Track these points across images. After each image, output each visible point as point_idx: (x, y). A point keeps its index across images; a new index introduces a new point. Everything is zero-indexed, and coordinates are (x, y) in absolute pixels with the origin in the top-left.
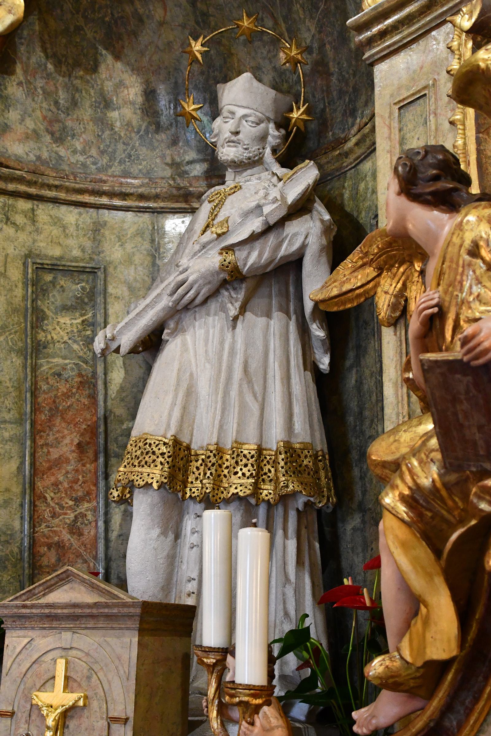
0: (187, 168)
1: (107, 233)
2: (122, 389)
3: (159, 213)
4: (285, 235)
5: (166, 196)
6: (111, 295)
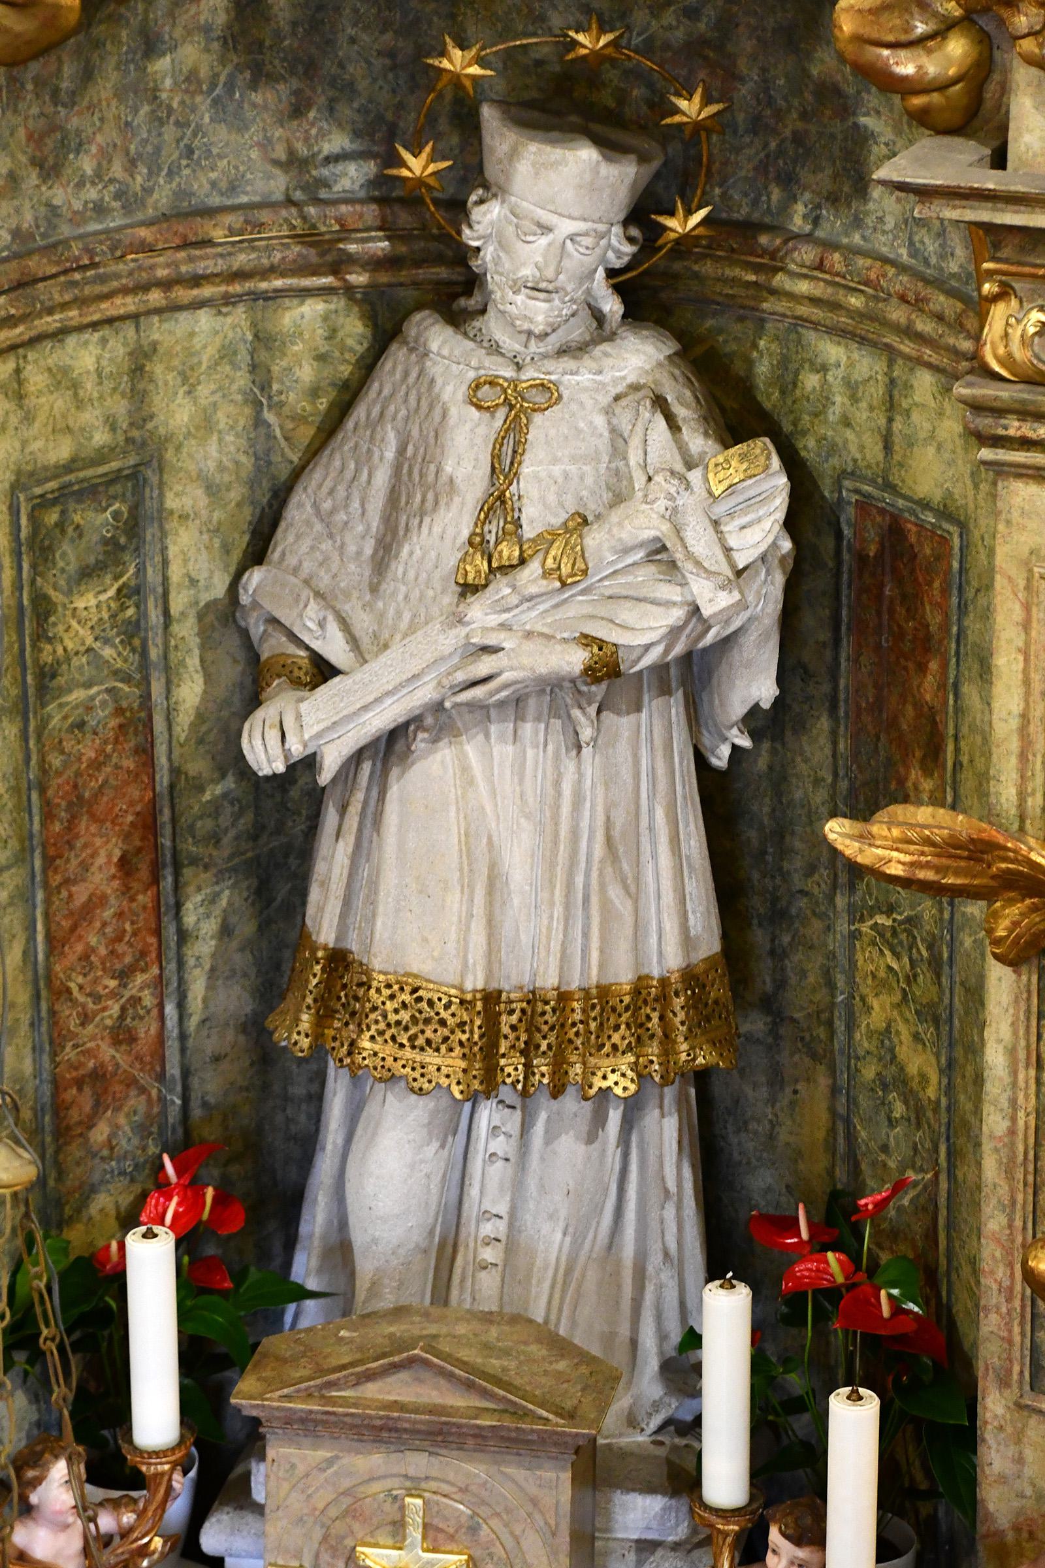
6: (172, 512)
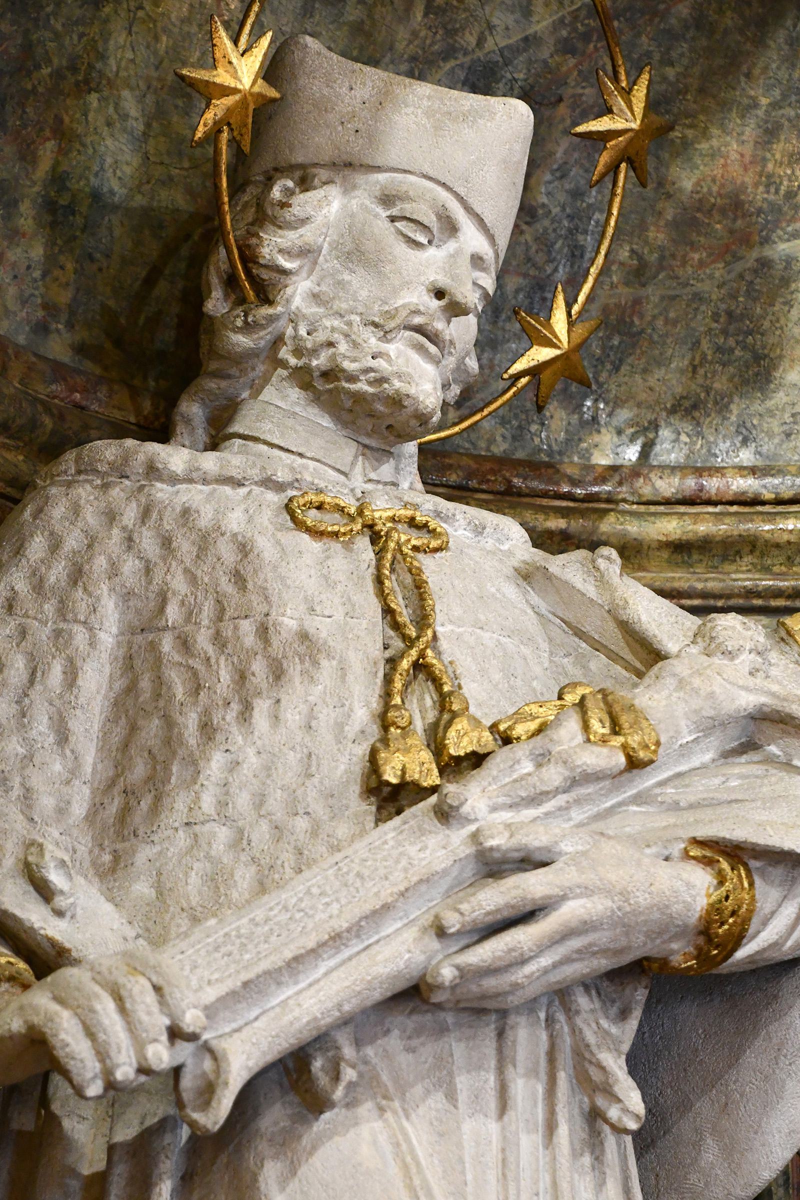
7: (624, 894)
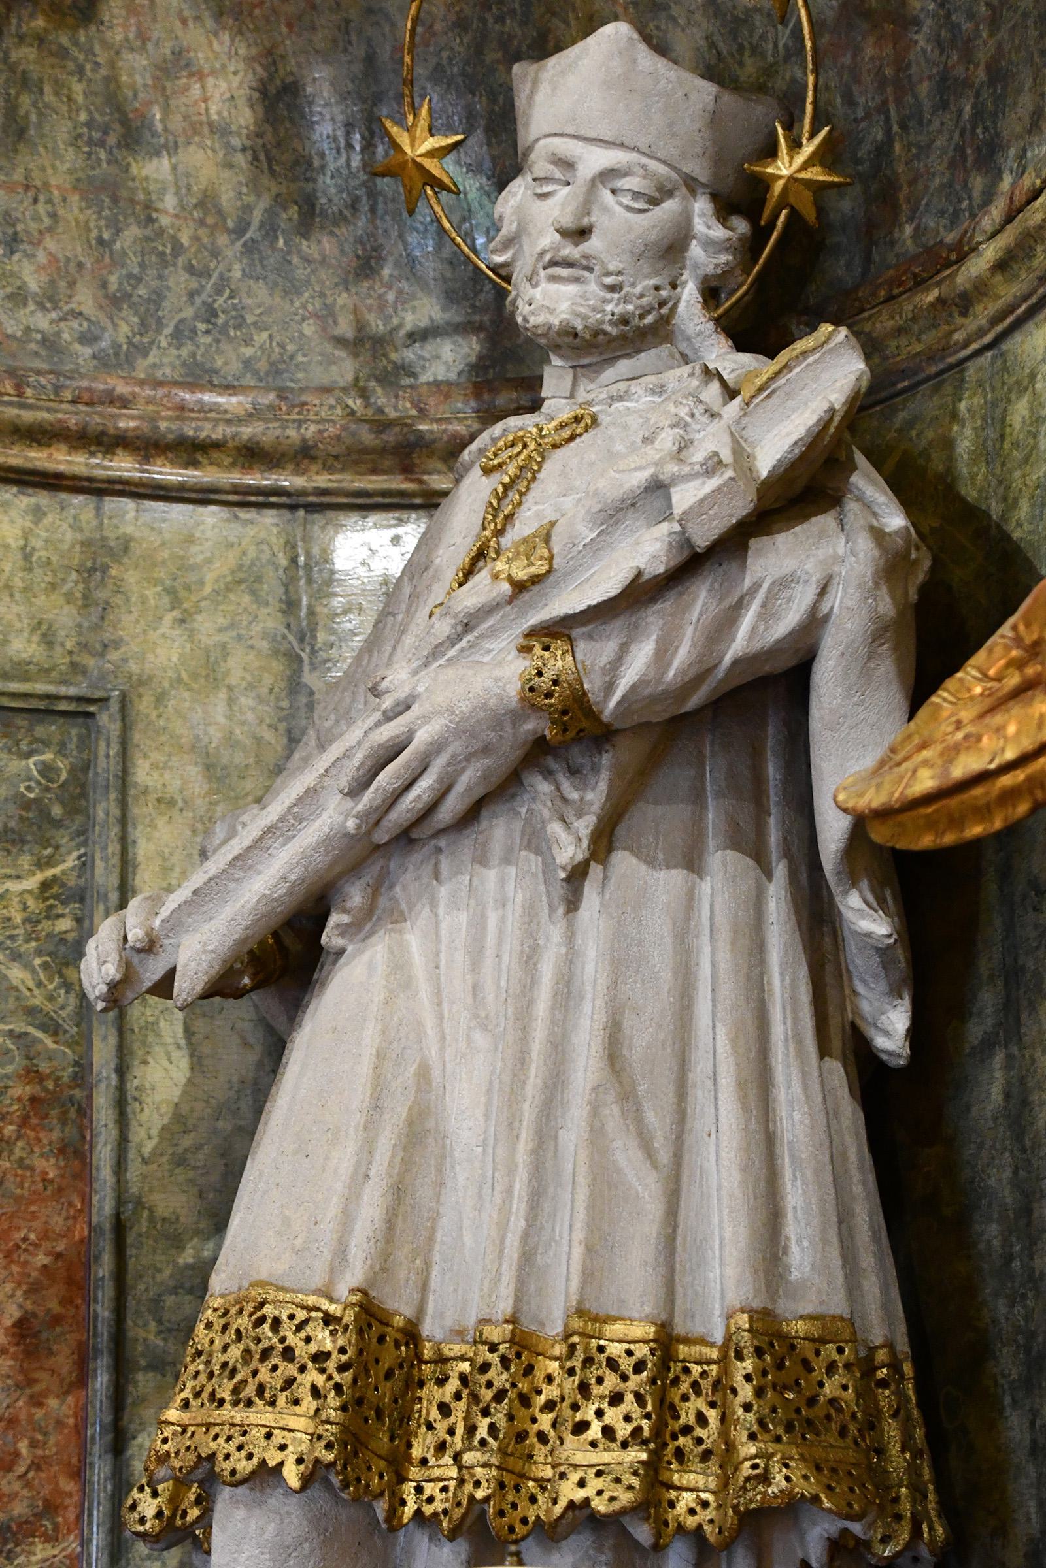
0: (409, 355)
1: (132, 578)
2: (179, 1122)
3: (311, 508)
4: (747, 583)
5: (335, 451)
6: (145, 792)
7: (450, 710)
